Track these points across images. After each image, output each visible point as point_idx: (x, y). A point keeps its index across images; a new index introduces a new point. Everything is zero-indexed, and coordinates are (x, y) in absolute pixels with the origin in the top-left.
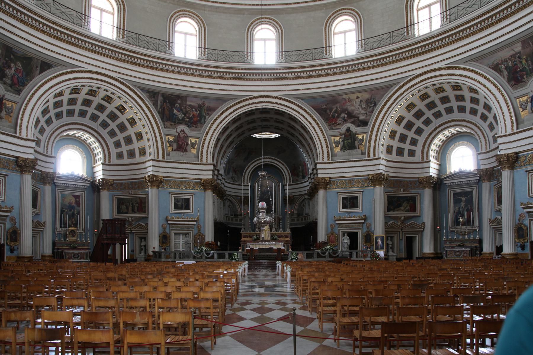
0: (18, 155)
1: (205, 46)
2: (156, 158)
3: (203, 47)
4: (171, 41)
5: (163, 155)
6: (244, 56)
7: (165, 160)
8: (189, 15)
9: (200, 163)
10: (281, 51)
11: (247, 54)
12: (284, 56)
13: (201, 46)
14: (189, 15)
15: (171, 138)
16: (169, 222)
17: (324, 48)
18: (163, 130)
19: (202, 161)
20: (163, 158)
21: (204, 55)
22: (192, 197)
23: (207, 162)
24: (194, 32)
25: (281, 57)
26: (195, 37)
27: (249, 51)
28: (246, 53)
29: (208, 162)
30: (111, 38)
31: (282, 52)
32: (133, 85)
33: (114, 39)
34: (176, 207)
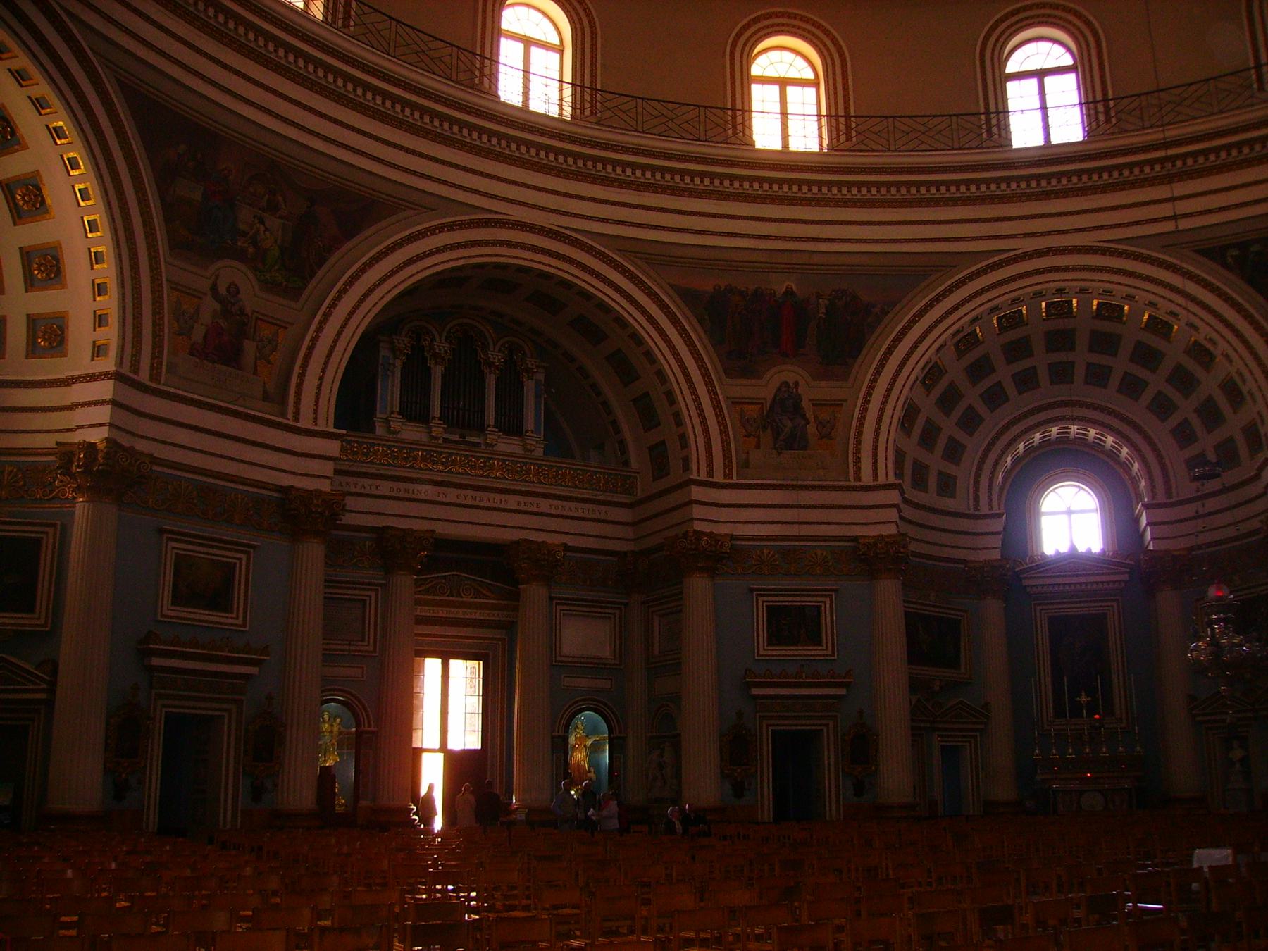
0: (287, 481)
1: (847, 107)
2: (703, 476)
3: (841, 112)
4: (739, 106)
5: (727, 466)
6: (980, 127)
7: (735, 480)
8: (788, 25)
9: (852, 483)
10: (1099, 97)
11: (988, 121)
12: (1113, 114)
13: (836, 109)
14: (788, 25)
15: (752, 411)
16: (755, 691)
17: (1253, 71)
18: (721, 383)
19: (858, 478)
20: (728, 475)
21: (849, 139)
22: (828, 600)
23: (876, 478)
24: (810, 75)
25: (1102, 117)
26: (812, 91)
27: (992, 109)
28: (983, 117)
29: (882, 479)
30: (554, 112)
31: (1105, 100)
32: (620, 251)
33: (568, 112)
34: (776, 638)
